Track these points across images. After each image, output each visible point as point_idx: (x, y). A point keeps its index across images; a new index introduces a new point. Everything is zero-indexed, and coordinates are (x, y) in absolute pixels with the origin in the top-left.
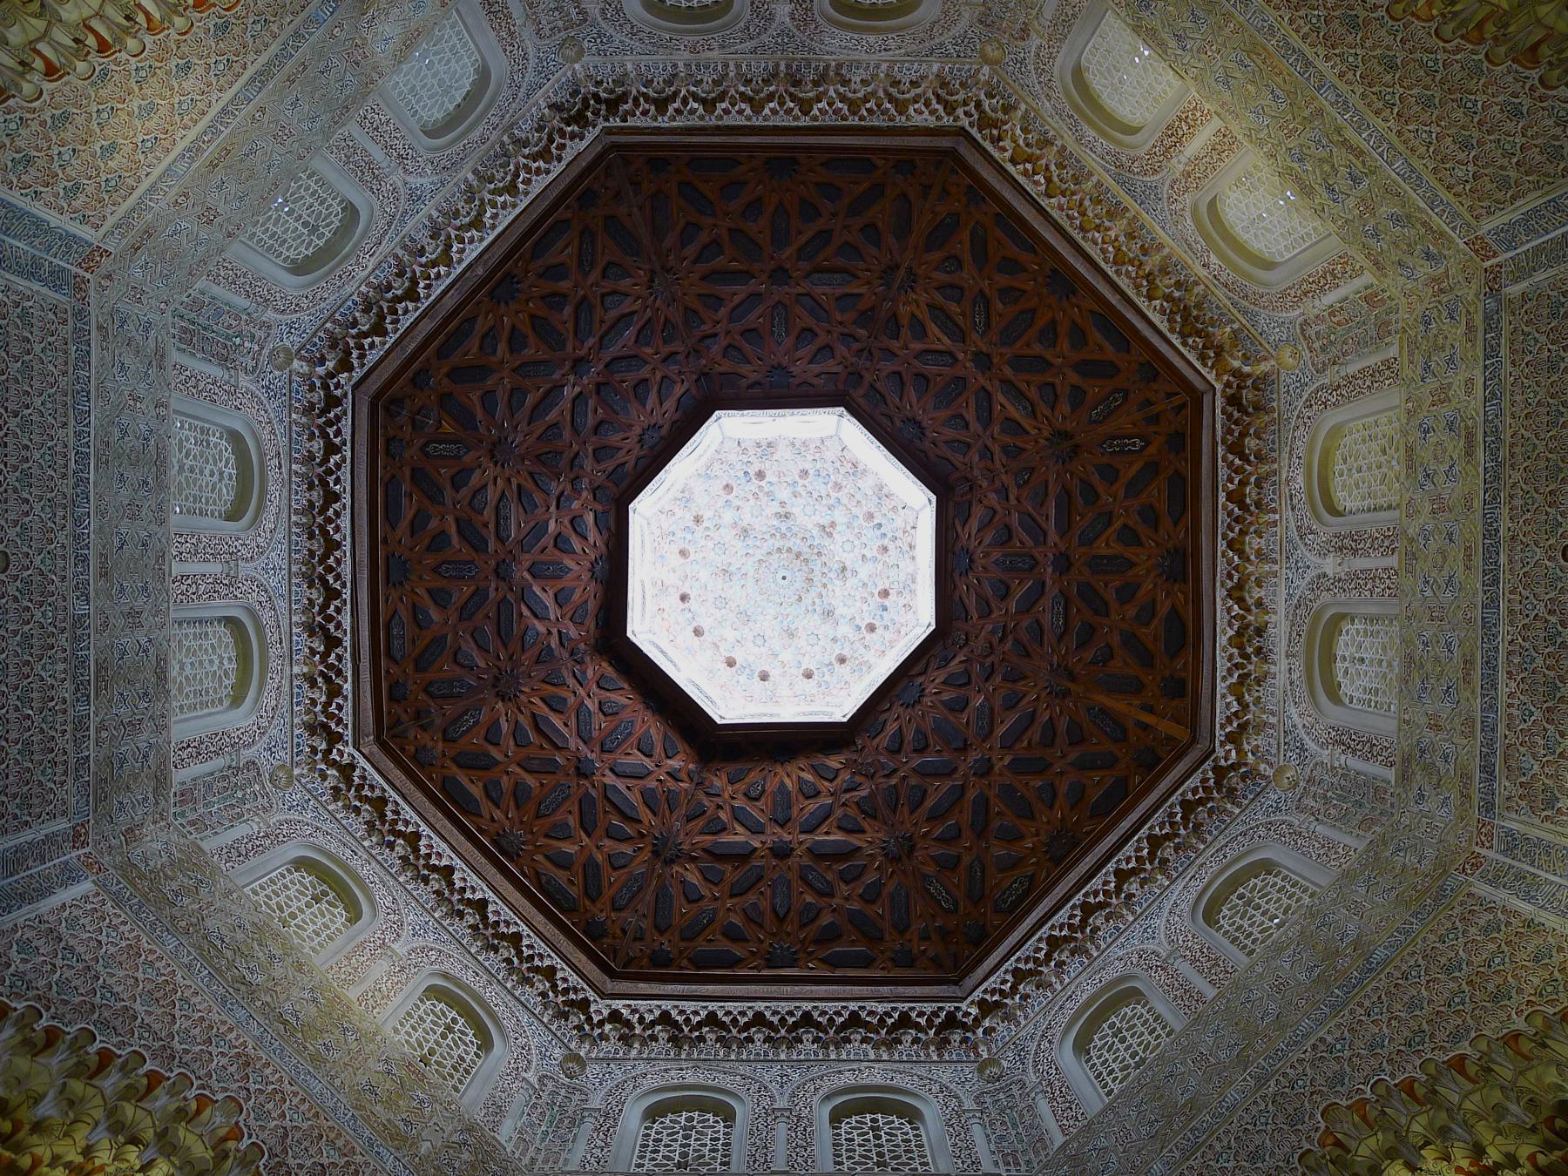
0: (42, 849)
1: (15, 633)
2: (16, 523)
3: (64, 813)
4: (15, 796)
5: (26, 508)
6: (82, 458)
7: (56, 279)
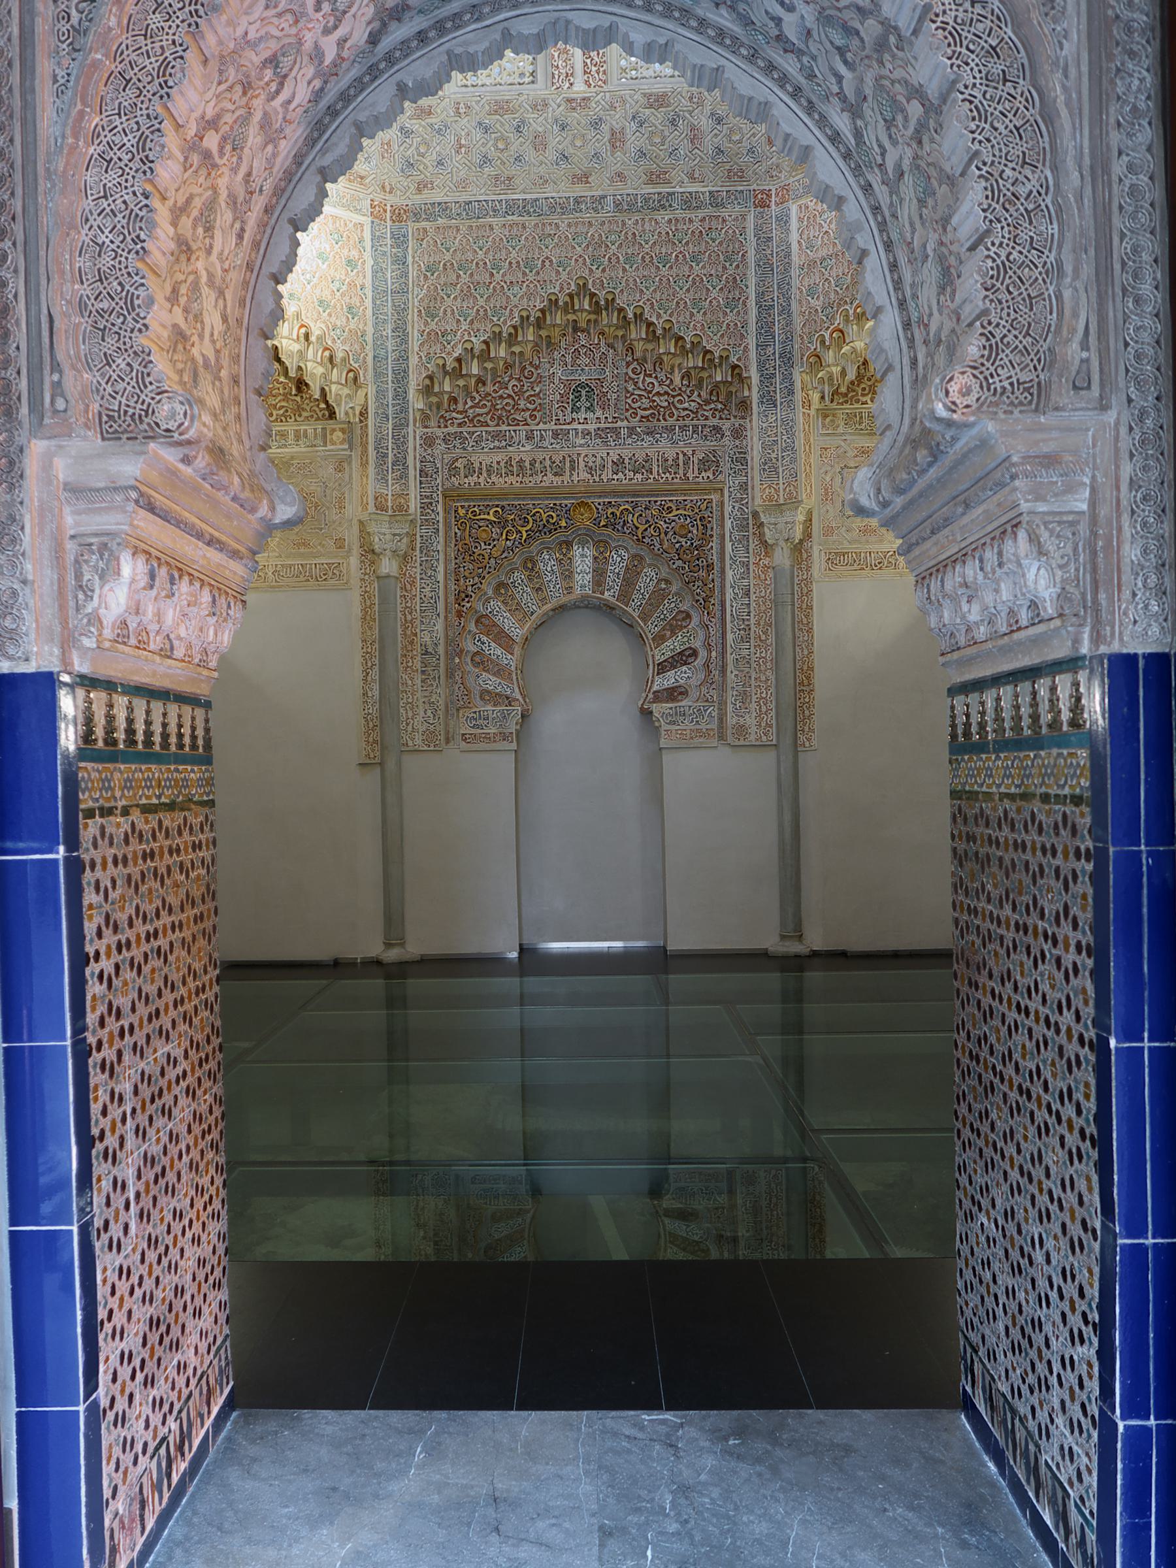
0: (764, 239)
1: (624, 270)
2: (558, 272)
3: (744, 217)
4: (725, 268)
5: (547, 263)
6: (511, 207)
7: (400, 240)
